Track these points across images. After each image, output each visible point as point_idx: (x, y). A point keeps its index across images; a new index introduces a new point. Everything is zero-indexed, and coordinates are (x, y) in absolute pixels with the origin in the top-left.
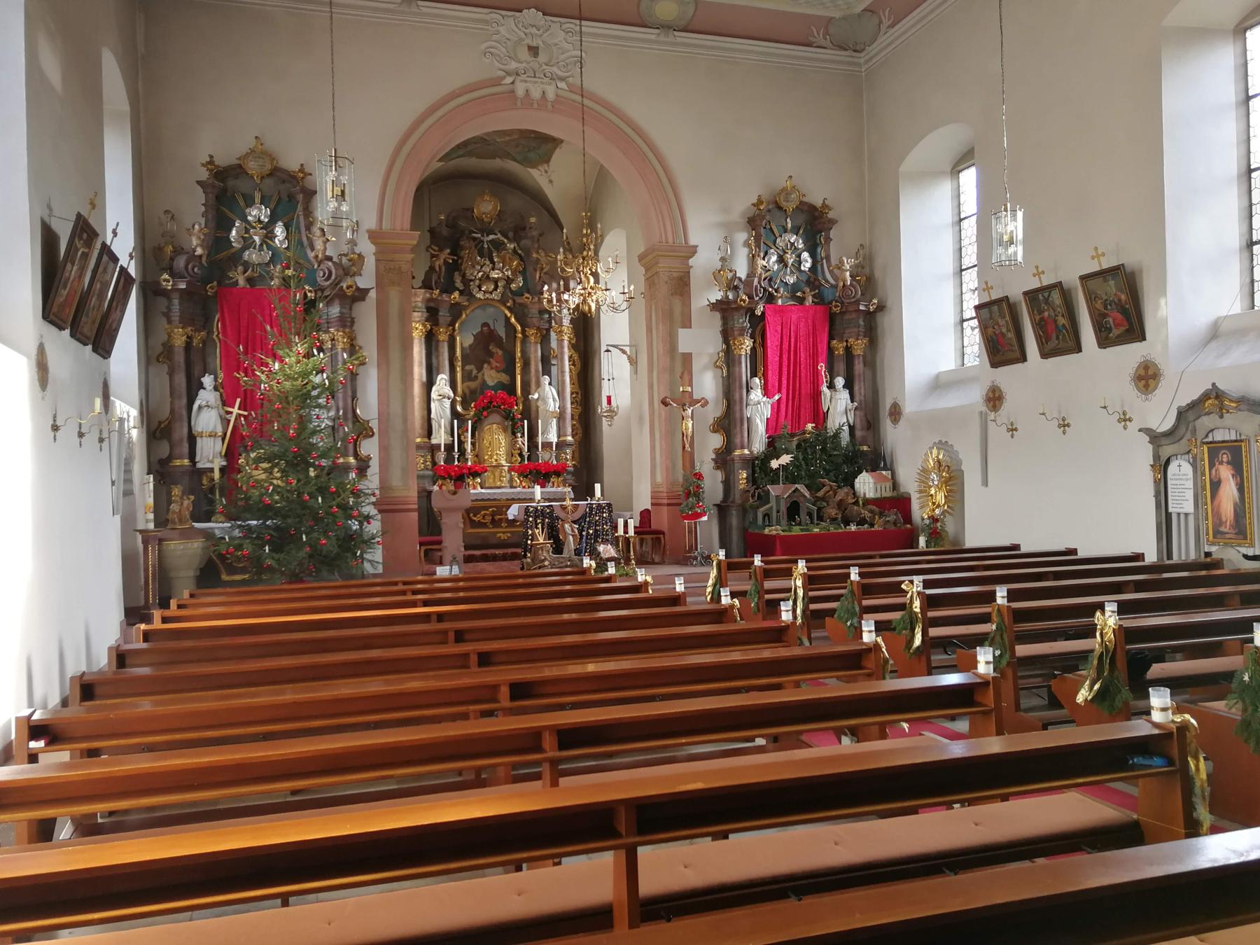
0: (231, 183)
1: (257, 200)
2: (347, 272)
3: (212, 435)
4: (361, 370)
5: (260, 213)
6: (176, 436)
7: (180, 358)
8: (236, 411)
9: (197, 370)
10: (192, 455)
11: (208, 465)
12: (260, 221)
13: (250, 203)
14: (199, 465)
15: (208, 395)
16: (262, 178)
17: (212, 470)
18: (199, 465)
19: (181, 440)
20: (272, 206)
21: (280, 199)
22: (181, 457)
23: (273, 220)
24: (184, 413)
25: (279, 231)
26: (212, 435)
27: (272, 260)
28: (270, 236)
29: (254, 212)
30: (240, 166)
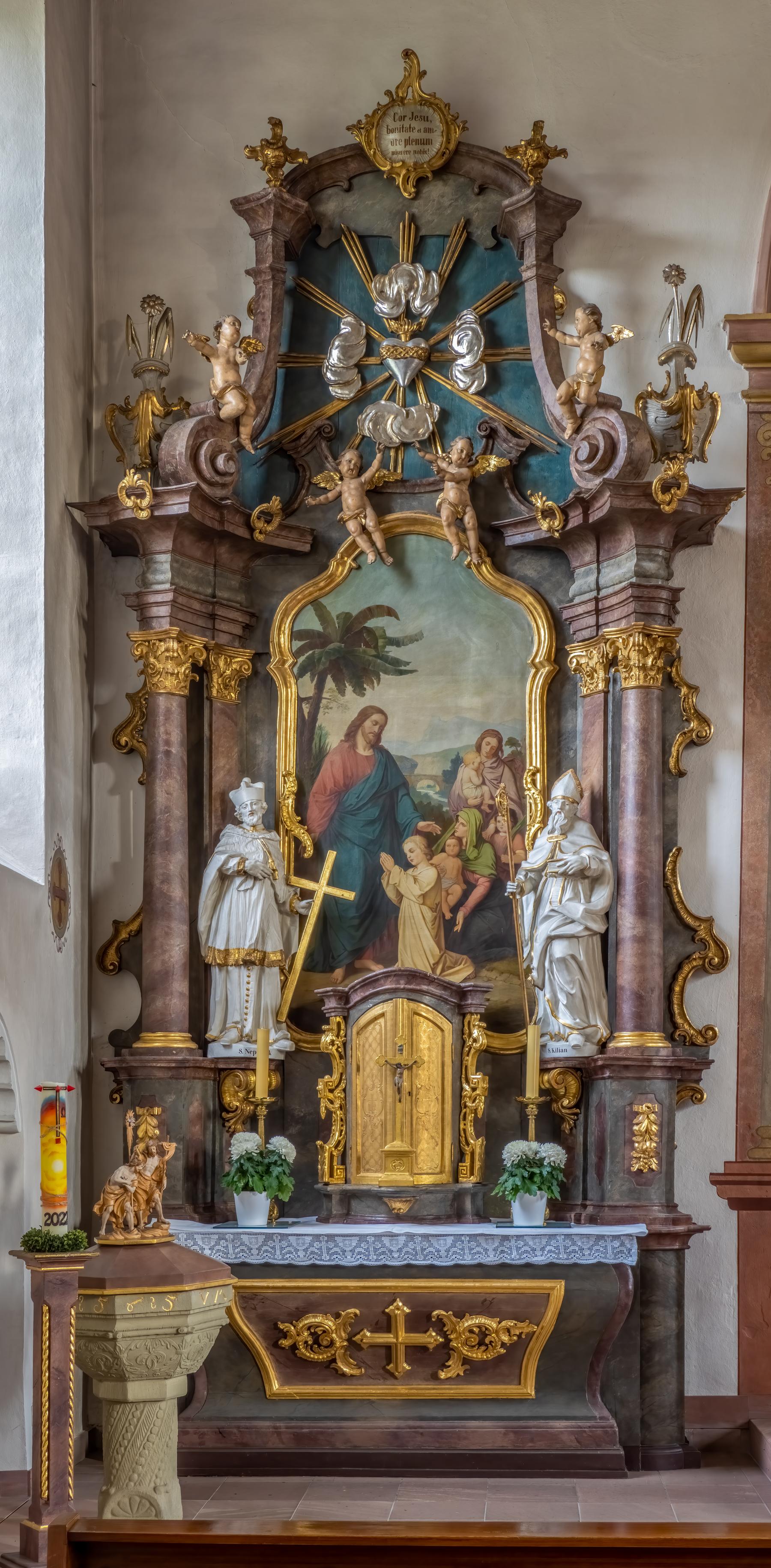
0: (333, 205)
1: (404, 251)
2: (673, 444)
3: (255, 961)
4: (692, 760)
5: (403, 288)
6: (153, 963)
7: (170, 732)
8: (322, 888)
9: (222, 765)
10: (198, 1023)
11: (238, 1050)
12: (409, 314)
13: (377, 253)
14: (216, 1051)
15: (245, 844)
16: (421, 182)
17: (247, 1064)
18: (216, 1051)
19: (166, 975)
20: (446, 266)
21: (469, 244)
22: (163, 1026)
23: (448, 304)
24: (178, 892)
26: (255, 961)
27: (439, 434)
28: (436, 359)
29: (395, 287)
30: (357, 152)
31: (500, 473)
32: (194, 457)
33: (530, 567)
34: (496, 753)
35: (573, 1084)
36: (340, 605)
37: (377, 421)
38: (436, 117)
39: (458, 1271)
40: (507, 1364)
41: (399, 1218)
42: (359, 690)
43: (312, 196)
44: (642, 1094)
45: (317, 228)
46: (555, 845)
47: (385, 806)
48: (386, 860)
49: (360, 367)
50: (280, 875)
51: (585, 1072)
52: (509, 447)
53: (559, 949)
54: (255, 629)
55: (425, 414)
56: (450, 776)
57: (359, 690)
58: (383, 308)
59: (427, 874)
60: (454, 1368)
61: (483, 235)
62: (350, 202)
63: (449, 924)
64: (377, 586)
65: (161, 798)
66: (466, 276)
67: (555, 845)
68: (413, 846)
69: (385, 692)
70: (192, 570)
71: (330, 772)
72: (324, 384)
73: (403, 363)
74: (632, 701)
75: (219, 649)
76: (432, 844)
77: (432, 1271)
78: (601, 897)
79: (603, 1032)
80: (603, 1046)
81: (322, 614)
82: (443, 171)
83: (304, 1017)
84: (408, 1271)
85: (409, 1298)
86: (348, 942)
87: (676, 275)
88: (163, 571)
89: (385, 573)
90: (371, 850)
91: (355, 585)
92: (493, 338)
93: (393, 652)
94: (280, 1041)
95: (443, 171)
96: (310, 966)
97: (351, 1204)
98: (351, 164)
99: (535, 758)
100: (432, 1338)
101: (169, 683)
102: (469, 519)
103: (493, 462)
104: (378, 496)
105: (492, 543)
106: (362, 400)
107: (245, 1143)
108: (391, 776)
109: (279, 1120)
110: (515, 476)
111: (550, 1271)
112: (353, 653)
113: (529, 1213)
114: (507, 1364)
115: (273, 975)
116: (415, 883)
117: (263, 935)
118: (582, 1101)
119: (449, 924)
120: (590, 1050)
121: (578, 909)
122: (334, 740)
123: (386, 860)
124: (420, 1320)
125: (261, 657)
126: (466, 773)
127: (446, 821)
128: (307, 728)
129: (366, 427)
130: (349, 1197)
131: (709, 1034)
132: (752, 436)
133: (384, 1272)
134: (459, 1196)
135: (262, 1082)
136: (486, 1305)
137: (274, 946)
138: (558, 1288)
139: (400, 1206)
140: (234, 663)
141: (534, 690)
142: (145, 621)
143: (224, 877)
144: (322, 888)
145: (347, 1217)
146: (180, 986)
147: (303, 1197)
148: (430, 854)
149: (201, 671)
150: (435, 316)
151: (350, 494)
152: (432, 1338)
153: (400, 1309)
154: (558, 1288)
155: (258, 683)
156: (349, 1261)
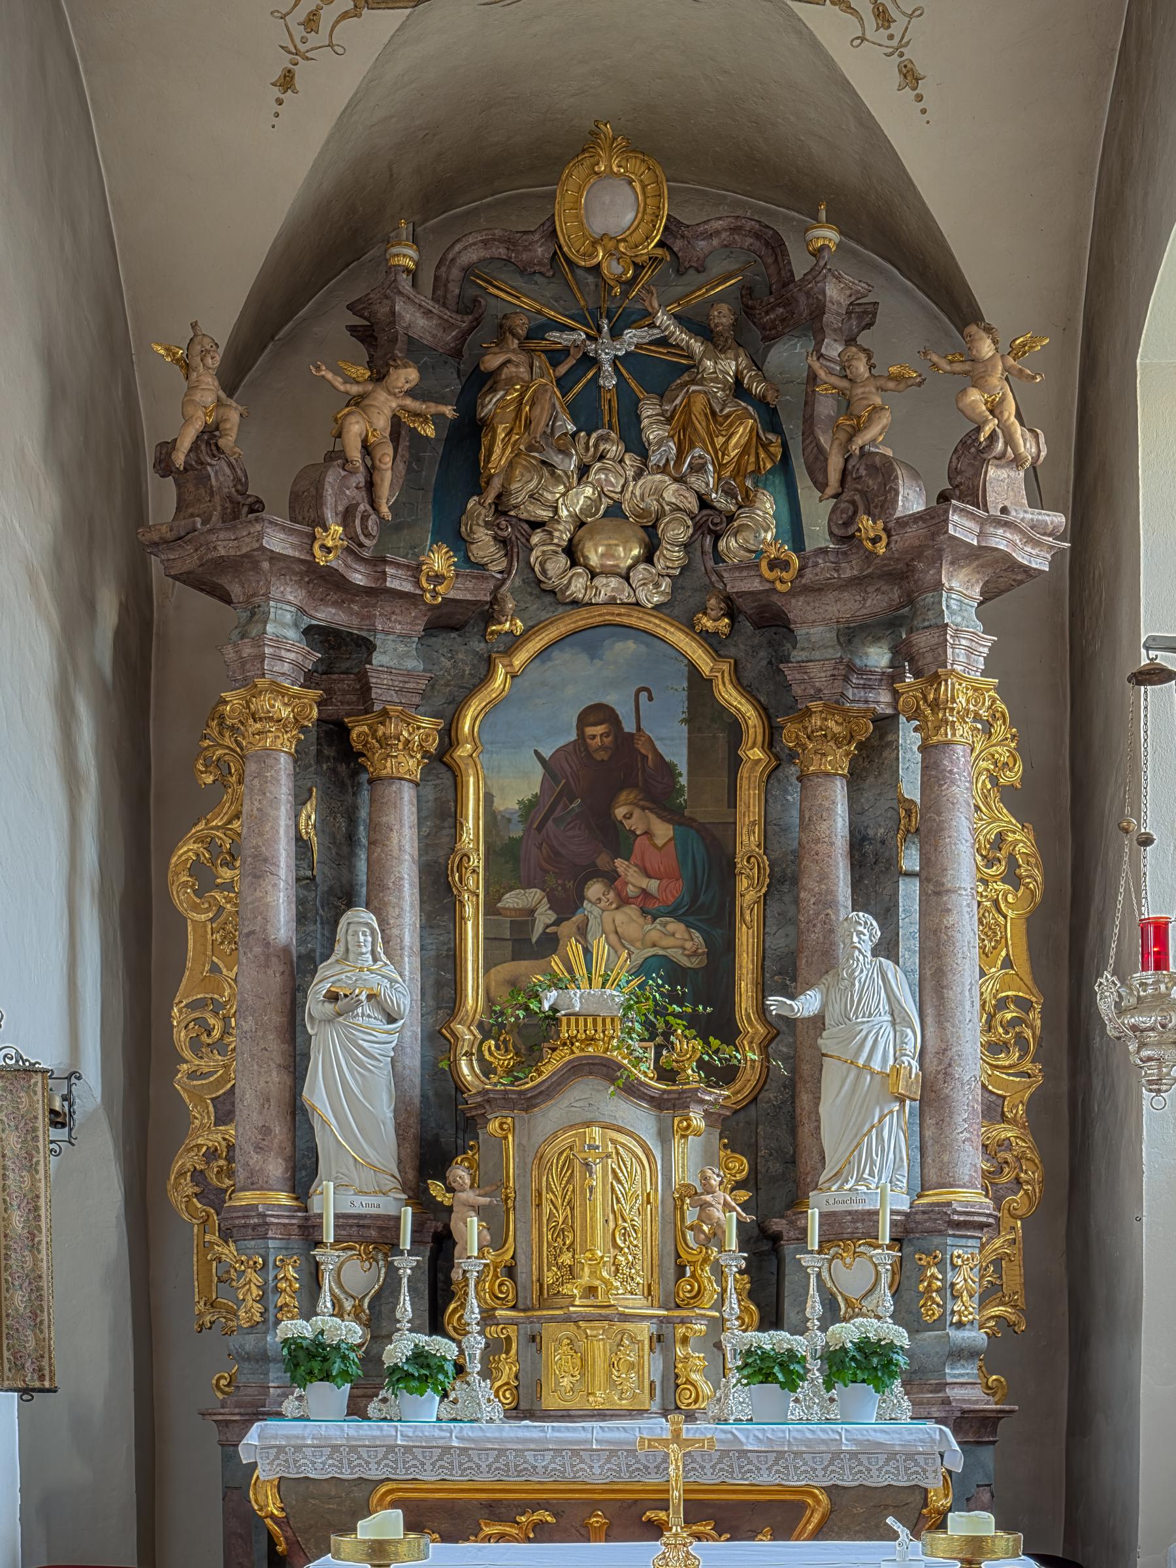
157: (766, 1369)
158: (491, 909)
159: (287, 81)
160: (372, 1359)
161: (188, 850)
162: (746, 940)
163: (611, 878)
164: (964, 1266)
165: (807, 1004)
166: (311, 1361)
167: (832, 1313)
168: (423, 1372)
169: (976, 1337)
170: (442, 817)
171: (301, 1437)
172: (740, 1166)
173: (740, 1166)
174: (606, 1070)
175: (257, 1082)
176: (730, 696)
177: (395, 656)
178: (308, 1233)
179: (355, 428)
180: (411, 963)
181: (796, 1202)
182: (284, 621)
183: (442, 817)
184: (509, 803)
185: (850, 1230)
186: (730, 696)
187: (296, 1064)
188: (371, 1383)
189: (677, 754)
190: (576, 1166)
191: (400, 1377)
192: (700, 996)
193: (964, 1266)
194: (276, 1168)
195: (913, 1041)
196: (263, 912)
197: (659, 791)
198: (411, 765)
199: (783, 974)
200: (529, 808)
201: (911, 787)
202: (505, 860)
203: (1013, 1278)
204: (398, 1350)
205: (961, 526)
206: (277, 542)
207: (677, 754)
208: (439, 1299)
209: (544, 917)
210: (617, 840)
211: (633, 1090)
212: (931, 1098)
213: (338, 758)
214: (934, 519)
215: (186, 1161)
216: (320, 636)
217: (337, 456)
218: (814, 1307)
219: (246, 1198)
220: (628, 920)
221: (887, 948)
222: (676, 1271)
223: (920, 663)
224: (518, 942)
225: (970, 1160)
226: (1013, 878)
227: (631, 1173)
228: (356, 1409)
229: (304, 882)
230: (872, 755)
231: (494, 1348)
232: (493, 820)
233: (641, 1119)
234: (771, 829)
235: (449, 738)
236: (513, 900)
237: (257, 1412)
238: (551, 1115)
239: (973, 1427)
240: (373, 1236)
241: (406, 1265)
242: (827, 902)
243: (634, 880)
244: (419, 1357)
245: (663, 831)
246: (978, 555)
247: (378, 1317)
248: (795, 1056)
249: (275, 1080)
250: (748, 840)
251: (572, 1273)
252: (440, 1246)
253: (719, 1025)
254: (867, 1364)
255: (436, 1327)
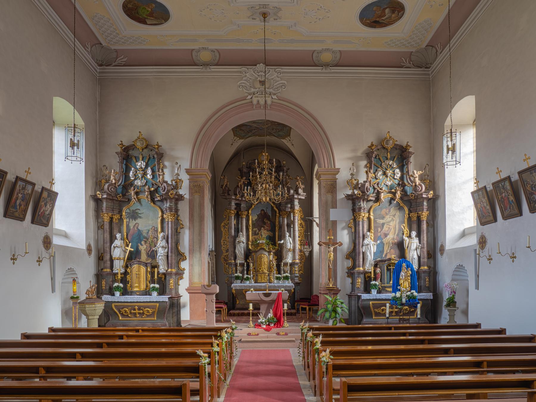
0: (131, 152)
1: (141, 159)
2: (176, 187)
3: (119, 259)
4: (182, 231)
5: (140, 164)
6: (105, 259)
7: (107, 227)
8: (129, 249)
9: (115, 231)
10: (112, 267)
11: (116, 272)
12: (142, 168)
13: (137, 160)
14: (114, 272)
15: (118, 242)
17: (117, 273)
18: (114, 272)
19: (106, 261)
20: (146, 161)
22: (106, 268)
23: (147, 166)
24: (108, 249)
25: (149, 171)
26: (119, 259)
27: (146, 184)
28: (145, 174)
29: (139, 164)
30: (134, 145)
31: (154, 190)
32: (108, 189)
33: (158, 203)
34: (154, 229)
35: (163, 276)
36: (132, 209)
37: (137, 183)
38: (144, 141)
39: (144, 302)
40: (152, 315)
41: (138, 295)
42: (135, 220)
43: (128, 151)
44: (171, 278)
45: (129, 155)
46: (161, 243)
47: (139, 237)
48: (139, 244)
49: (135, 175)
50: (123, 247)
51: (164, 274)
52: (155, 187)
53: (160, 257)
54: (120, 212)
55: (144, 181)
56: (148, 233)
57: (135, 220)
58: (138, 167)
59: (145, 246)
60: (145, 316)
61: (151, 157)
62: (133, 152)
63: (148, 254)
64: (137, 206)
65: (105, 236)
66: (149, 162)
67: (161, 243)
68: (143, 242)
69: (139, 221)
70: (110, 204)
71: (131, 232)
72: (130, 177)
73: (140, 174)
74: (170, 223)
75: (114, 215)
76: (145, 242)
77: (140, 302)
78: (166, 250)
79: (167, 269)
80: (167, 271)
81: (130, 210)
82: (146, 148)
83: (127, 267)
84: (137, 302)
85: (137, 306)
86: (133, 257)
87: (177, 163)
88: (105, 205)
89: (138, 204)
90: (137, 243)
91: (134, 205)
92: (153, 171)
93: (140, 215)
94: (123, 271)
95: (146, 148)
96: (128, 259)
97: (132, 293)
98: (132, 147)
99: (159, 230)
100: (141, 311)
101: (106, 220)
102: (149, 197)
103: (152, 189)
104: (137, 193)
105: (153, 200)
106: (135, 179)
107: (116, 284)
108: (140, 233)
109: (121, 282)
110: (156, 190)
111: (156, 302)
112: (134, 215)
113: (155, 294)
114: (152, 315)
115: (122, 261)
116: (143, 248)
117: (120, 255)
118: (165, 278)
119: (148, 254)
120: (165, 271)
121: (162, 252)
122: (132, 228)
123: (139, 244)
124: (139, 309)
125: (121, 216)
126: (150, 232)
127: (147, 239)
128: (128, 226)
129: (136, 183)
130: (132, 292)
131: (184, 269)
132: (190, 185)
133: (134, 302)
134: (146, 292)
135: (119, 276)
136: (148, 307)
137: (122, 257)
138: (158, 304)
139: (138, 293)
140: (116, 217)
141: (159, 220)
142: (102, 212)
143: (115, 247)
144: (129, 249)
145: (131, 295)
146: (109, 263)
147: (125, 292)
148: (145, 244)
149: (112, 218)
150: (145, 168)
151: (133, 193)
152: (141, 311)
153: (136, 307)
154: (158, 304)
155: (121, 220)
156: (129, 301)
157: (278, 278)
158: (252, 230)
159: (232, 144)
160: (243, 277)
161: (223, 224)
162: (277, 233)
163: (264, 227)
164: (297, 268)
165: (282, 242)
166: (237, 278)
167: (285, 273)
168: (248, 279)
169: (298, 275)
170: (248, 221)
171: (236, 285)
172: (276, 257)
173: (276, 257)
174: (264, 249)
175: (231, 250)
176: (275, 208)
177: (243, 205)
178: (236, 265)
179: (240, 184)
180: (245, 237)
181: (281, 261)
182: (233, 204)
183: (248, 221)
184: (254, 219)
185: (285, 264)
186: (275, 208)
187: (235, 248)
188: (242, 280)
189: (270, 215)
190: (261, 258)
191: (245, 279)
192: (272, 240)
193: (297, 268)
194: (233, 258)
195: (292, 246)
196: (231, 232)
197: (269, 219)
198: (245, 216)
199: (280, 239)
200: (256, 220)
201: (292, 219)
202: (253, 225)
203: (302, 269)
204: (245, 276)
205: (296, 196)
206: (233, 197)
207: (270, 215)
208: (248, 270)
209: (257, 231)
210: (265, 223)
211: (266, 251)
212: (294, 251)
213: (238, 216)
214: (293, 196)
215: (223, 257)
216: (236, 204)
217: (238, 186)
218: (282, 272)
219: (230, 261)
220: (265, 231)
221: (290, 236)
222: (270, 269)
223: (293, 208)
224: (254, 234)
225: (297, 257)
226: (302, 227)
227: (267, 258)
228: (241, 283)
229: (235, 228)
230: (289, 216)
231: (253, 276)
232: (252, 221)
233: (267, 254)
234: (279, 222)
235: (248, 213)
236: (254, 229)
237: (232, 283)
238: (258, 253)
239: (296, 284)
240: (242, 265)
241: (245, 268)
242: (284, 230)
243: (266, 227)
244: (247, 277)
245: (269, 222)
246: (298, 198)
247: (242, 272)
248: (281, 246)
249: (233, 249)
250: (277, 223)
251: (260, 269)
252: (248, 266)
253: (274, 244)
254: (286, 278)
255: (247, 274)
